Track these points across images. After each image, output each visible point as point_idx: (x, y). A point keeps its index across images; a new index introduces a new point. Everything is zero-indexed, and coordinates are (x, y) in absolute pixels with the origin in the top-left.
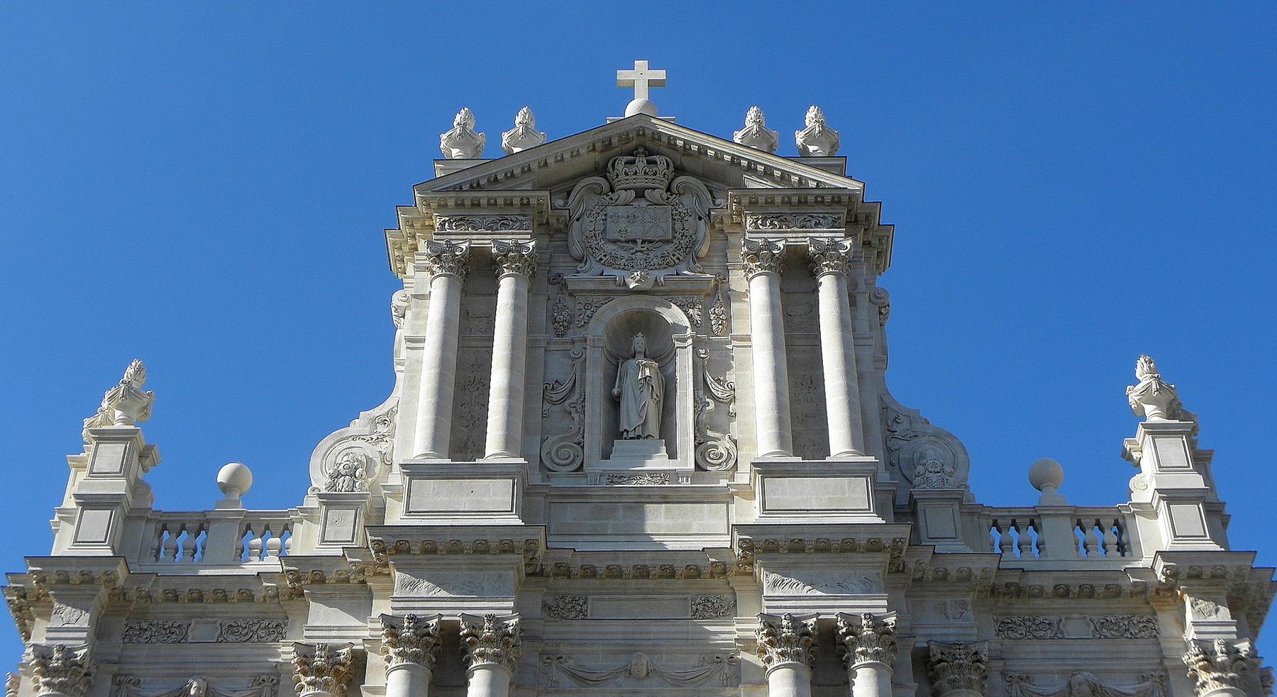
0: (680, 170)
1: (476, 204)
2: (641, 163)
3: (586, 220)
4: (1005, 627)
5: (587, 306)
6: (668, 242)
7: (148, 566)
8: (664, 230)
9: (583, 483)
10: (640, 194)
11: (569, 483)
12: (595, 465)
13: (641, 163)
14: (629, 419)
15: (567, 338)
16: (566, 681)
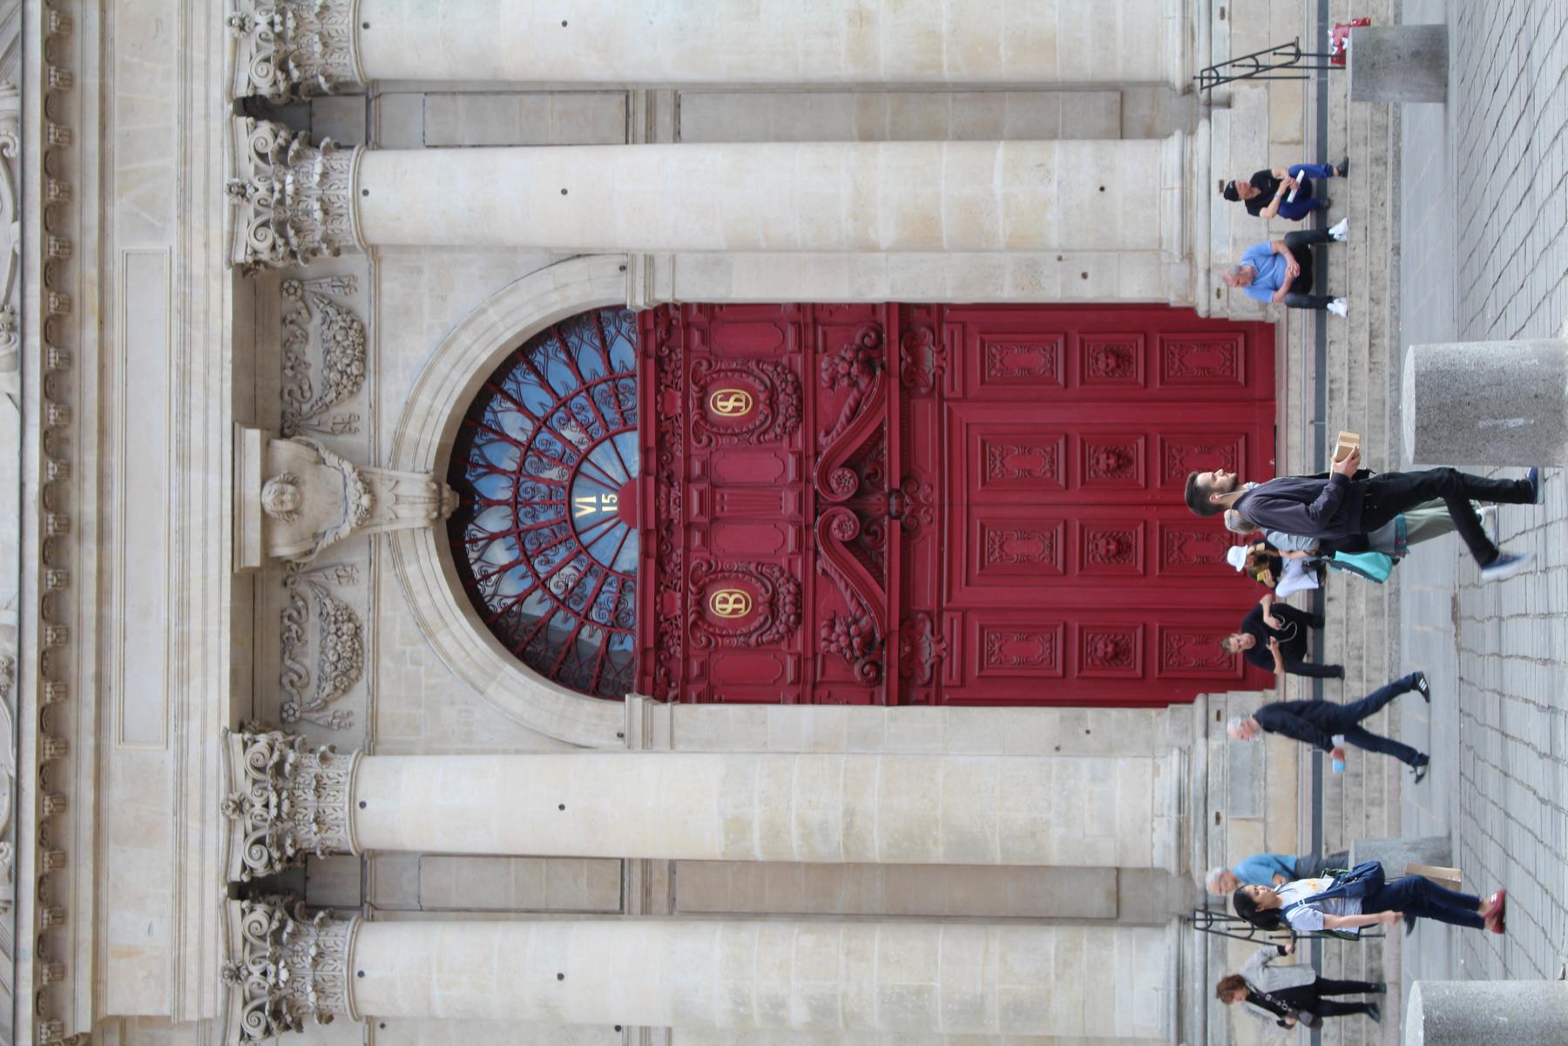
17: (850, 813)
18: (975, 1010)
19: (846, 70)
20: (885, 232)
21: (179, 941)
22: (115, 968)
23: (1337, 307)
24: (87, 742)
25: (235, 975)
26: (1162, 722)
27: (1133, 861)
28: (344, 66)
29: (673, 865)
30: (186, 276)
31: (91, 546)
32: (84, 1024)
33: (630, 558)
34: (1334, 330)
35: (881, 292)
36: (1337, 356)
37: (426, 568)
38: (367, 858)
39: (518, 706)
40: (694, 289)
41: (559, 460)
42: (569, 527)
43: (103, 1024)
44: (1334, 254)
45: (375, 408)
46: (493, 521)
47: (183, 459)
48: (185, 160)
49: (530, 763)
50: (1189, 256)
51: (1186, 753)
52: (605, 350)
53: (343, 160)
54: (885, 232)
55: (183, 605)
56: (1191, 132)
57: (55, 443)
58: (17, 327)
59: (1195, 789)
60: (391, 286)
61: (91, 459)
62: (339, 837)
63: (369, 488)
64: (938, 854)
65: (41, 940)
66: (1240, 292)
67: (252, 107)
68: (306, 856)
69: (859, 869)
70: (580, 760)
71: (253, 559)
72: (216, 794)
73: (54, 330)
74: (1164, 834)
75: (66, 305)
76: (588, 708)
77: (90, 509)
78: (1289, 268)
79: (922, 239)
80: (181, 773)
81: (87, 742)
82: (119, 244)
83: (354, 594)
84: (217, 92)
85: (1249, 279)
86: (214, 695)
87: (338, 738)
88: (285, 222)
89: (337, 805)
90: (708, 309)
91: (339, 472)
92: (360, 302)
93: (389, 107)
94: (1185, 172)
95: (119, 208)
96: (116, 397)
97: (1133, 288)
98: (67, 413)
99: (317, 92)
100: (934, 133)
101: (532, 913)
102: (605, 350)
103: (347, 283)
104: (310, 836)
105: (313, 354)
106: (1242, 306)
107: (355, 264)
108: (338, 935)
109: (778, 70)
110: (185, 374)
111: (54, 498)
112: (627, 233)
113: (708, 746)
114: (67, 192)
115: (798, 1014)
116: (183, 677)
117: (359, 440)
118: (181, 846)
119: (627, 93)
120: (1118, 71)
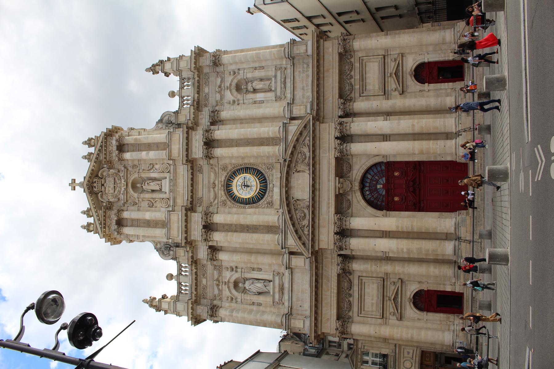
0: (97, 176)
1: (105, 224)
2: (95, 185)
3: (109, 198)
4: (206, 106)
5: (130, 197)
6: (115, 179)
7: (189, 295)
8: (112, 179)
9: (172, 198)
10: (103, 185)
11: (172, 201)
12: (167, 196)
13: (95, 185)
14: (157, 188)
15: (137, 202)
16: (216, 202)
17: (412, 225)
18: (428, 250)
19: (411, 132)
20: (417, 152)
21: (328, 239)
22: (321, 242)
23: (476, 161)
24: (317, 215)
25: (335, 244)
26: (453, 214)
27: (449, 232)
28: (348, 133)
29: (389, 231)
30: (329, 159)
31: (318, 191)
32: (317, 249)
33: (384, 193)
34: (476, 164)
35: (416, 159)
36: (476, 167)
37: (358, 195)
38: (351, 230)
39: (370, 211)
40: (392, 159)
41: (375, 181)
42: (376, 189)
43: (319, 249)
44: (476, 154)
45: (352, 175)
46: (367, 189)
47: (329, 181)
48: (329, 145)
49: (372, 219)
50: (456, 155)
51: (456, 218)
52: (381, 167)
53: (348, 144)
54: (417, 152)
55: (329, 199)
56: (456, 139)
57: (314, 179)
58: (309, 165)
59: (457, 223)
60: (354, 160)
61: (318, 181)
62: (348, 227)
63: (351, 184)
64: (423, 231)
65: (312, 239)
66: (463, 159)
67: (337, 138)
68: (344, 230)
69: (413, 232)
70: (378, 218)
71: (337, 193)
72: (333, 222)
73: (314, 165)
74: (453, 229)
75: (315, 162)
76: (379, 212)
77: (318, 187)
78: (470, 156)
79: (421, 153)
80: (329, 219)
81: (317, 215)
82: (321, 155)
83: (350, 198)
84: (333, 137)
85: (464, 156)
86: (332, 209)
87: (348, 215)
88: (341, 152)
89: (348, 223)
90: (394, 162)
91: (348, 183)
92: (350, 162)
93: (354, 138)
94: (456, 144)
95: (321, 151)
96: (321, 173)
97: (449, 159)
98: (315, 176)
99: (345, 136)
100: (422, 139)
101: (371, 237)
102: (381, 167)
103: (349, 159)
104: (344, 227)
105: (345, 168)
106: (463, 160)
107: (350, 157)
108: (348, 239)
109: (403, 132)
110: (329, 171)
111: (314, 186)
112: (383, 153)
113: (394, 217)
114: (315, 149)
115: (405, 250)
116: (329, 207)
117: (350, 179)
118: (329, 228)
119: (383, 135)
120: (447, 131)
